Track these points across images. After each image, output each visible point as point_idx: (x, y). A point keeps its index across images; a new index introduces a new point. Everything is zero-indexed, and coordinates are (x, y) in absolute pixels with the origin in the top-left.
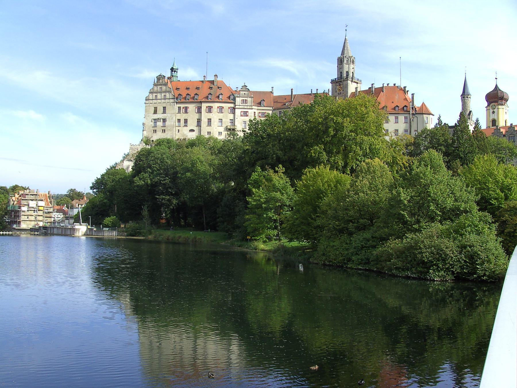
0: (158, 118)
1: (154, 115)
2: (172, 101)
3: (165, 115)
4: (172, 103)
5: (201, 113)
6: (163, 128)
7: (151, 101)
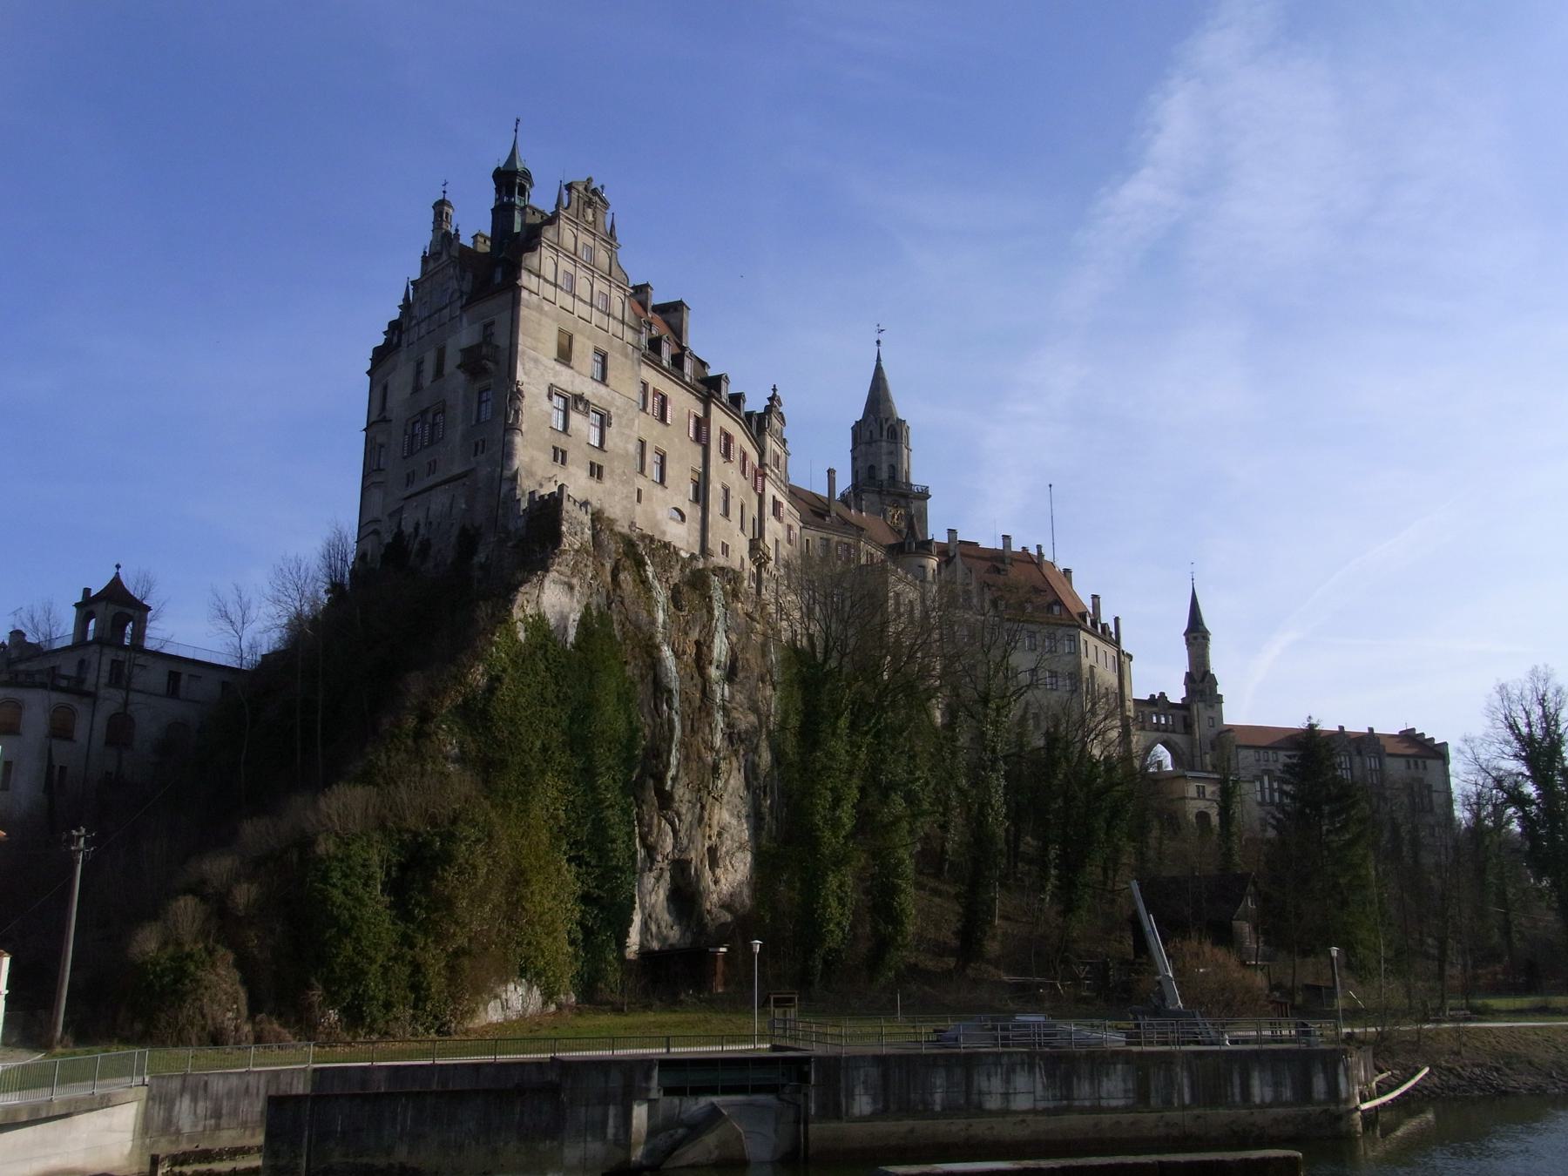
0: (578, 391)
1: (559, 367)
2: (629, 336)
3: (602, 389)
7: (549, 291)
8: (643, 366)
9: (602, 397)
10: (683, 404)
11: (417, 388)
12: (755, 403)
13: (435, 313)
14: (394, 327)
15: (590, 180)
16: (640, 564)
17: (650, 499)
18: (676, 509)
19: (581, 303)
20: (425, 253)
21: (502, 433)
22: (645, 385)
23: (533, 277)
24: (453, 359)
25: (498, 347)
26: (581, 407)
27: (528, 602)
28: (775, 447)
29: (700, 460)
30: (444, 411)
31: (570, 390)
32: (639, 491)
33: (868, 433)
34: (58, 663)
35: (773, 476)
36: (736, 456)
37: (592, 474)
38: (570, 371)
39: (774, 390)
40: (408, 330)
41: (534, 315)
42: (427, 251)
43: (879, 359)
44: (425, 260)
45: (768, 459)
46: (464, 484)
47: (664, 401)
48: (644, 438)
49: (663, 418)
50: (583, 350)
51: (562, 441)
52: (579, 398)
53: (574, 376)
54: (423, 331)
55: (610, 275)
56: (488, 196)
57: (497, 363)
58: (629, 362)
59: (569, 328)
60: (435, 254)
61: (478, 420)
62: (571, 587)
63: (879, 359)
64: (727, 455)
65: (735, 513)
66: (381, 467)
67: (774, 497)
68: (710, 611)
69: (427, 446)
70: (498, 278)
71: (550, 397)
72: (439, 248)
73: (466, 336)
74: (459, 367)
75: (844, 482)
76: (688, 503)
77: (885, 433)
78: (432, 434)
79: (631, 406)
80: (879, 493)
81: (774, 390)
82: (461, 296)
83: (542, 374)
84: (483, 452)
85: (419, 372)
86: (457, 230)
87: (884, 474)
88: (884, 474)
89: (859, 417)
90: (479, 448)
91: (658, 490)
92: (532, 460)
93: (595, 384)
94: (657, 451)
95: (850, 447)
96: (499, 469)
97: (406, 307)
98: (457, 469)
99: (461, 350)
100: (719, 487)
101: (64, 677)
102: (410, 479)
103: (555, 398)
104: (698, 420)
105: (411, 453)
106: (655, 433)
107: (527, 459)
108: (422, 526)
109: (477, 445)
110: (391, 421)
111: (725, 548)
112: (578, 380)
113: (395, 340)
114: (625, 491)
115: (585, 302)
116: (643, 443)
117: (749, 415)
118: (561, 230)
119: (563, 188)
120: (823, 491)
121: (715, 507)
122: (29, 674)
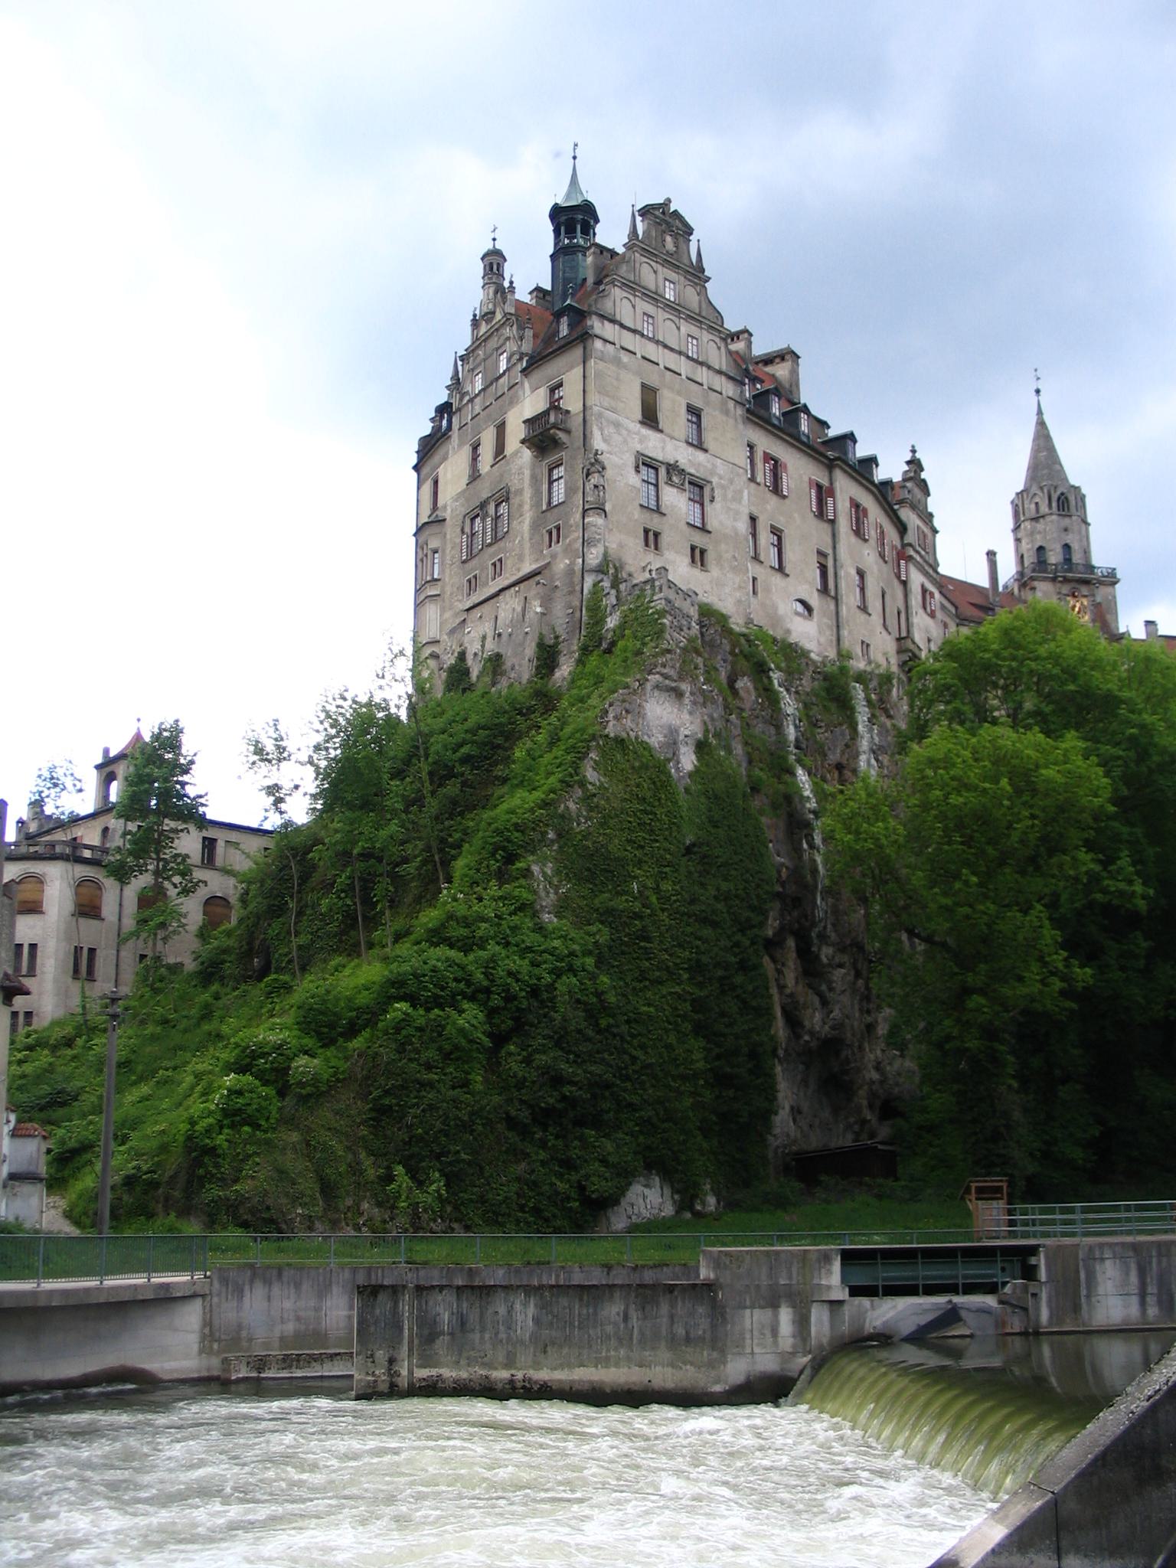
1: (646, 431)
2: (729, 389)
3: (701, 456)
4: (731, 404)
5: (832, 522)
6: (699, 539)
7: (629, 340)
8: (750, 426)
9: (699, 464)
10: (800, 471)
11: (475, 476)
12: (890, 469)
13: (491, 384)
14: (444, 410)
15: (669, 200)
16: (760, 670)
17: (768, 590)
18: (802, 602)
19: (666, 351)
20: (475, 315)
21: (578, 516)
22: (751, 446)
23: (606, 323)
24: (516, 432)
25: (568, 412)
26: (675, 479)
27: (627, 712)
28: (918, 522)
29: (829, 540)
30: (508, 499)
31: (660, 458)
32: (754, 579)
33: (1033, 506)
34: (79, 834)
35: (918, 558)
36: (872, 534)
37: (693, 561)
38: (659, 435)
39: (914, 451)
40: (459, 410)
41: (610, 369)
42: (478, 312)
43: (1040, 412)
44: (475, 323)
45: (911, 537)
46: (538, 583)
47: (777, 468)
48: (756, 513)
49: (776, 489)
50: (672, 407)
51: (655, 523)
52: (673, 468)
53: (664, 441)
54: (478, 409)
55: (699, 315)
56: (545, 238)
57: (568, 432)
58: (731, 421)
59: (653, 380)
60: (486, 314)
61: (549, 503)
62: (679, 694)
63: (1040, 412)
64: (858, 532)
65: (874, 604)
66: (436, 576)
67: (923, 586)
68: (853, 726)
69: (490, 545)
70: (564, 330)
71: (637, 470)
72: (491, 306)
73: (531, 402)
74: (523, 442)
75: (1007, 570)
76: (816, 594)
77: (1054, 504)
78: (495, 529)
79: (738, 475)
80: (1054, 580)
81: (914, 451)
82: (520, 359)
83: (625, 441)
84: (558, 542)
85: (475, 458)
86: (511, 282)
87: (1054, 557)
88: (1054, 557)
89: (1020, 487)
90: (555, 534)
91: (777, 579)
92: (621, 546)
93: (691, 449)
94: (776, 532)
95: (1010, 523)
96: (580, 560)
97: (456, 384)
98: (528, 568)
99: (524, 422)
100: (853, 572)
101: (87, 847)
102: (472, 584)
103: (644, 469)
104: (819, 487)
105: (471, 556)
106: (769, 507)
107: (614, 546)
108: (489, 639)
109: (550, 533)
110: (444, 520)
111: (865, 645)
112: (670, 445)
113: (444, 422)
114: (737, 580)
115: (672, 350)
116: (753, 519)
117: (887, 484)
118: (637, 265)
119: (637, 214)
120: (984, 582)
121: (850, 598)
122: (53, 845)
